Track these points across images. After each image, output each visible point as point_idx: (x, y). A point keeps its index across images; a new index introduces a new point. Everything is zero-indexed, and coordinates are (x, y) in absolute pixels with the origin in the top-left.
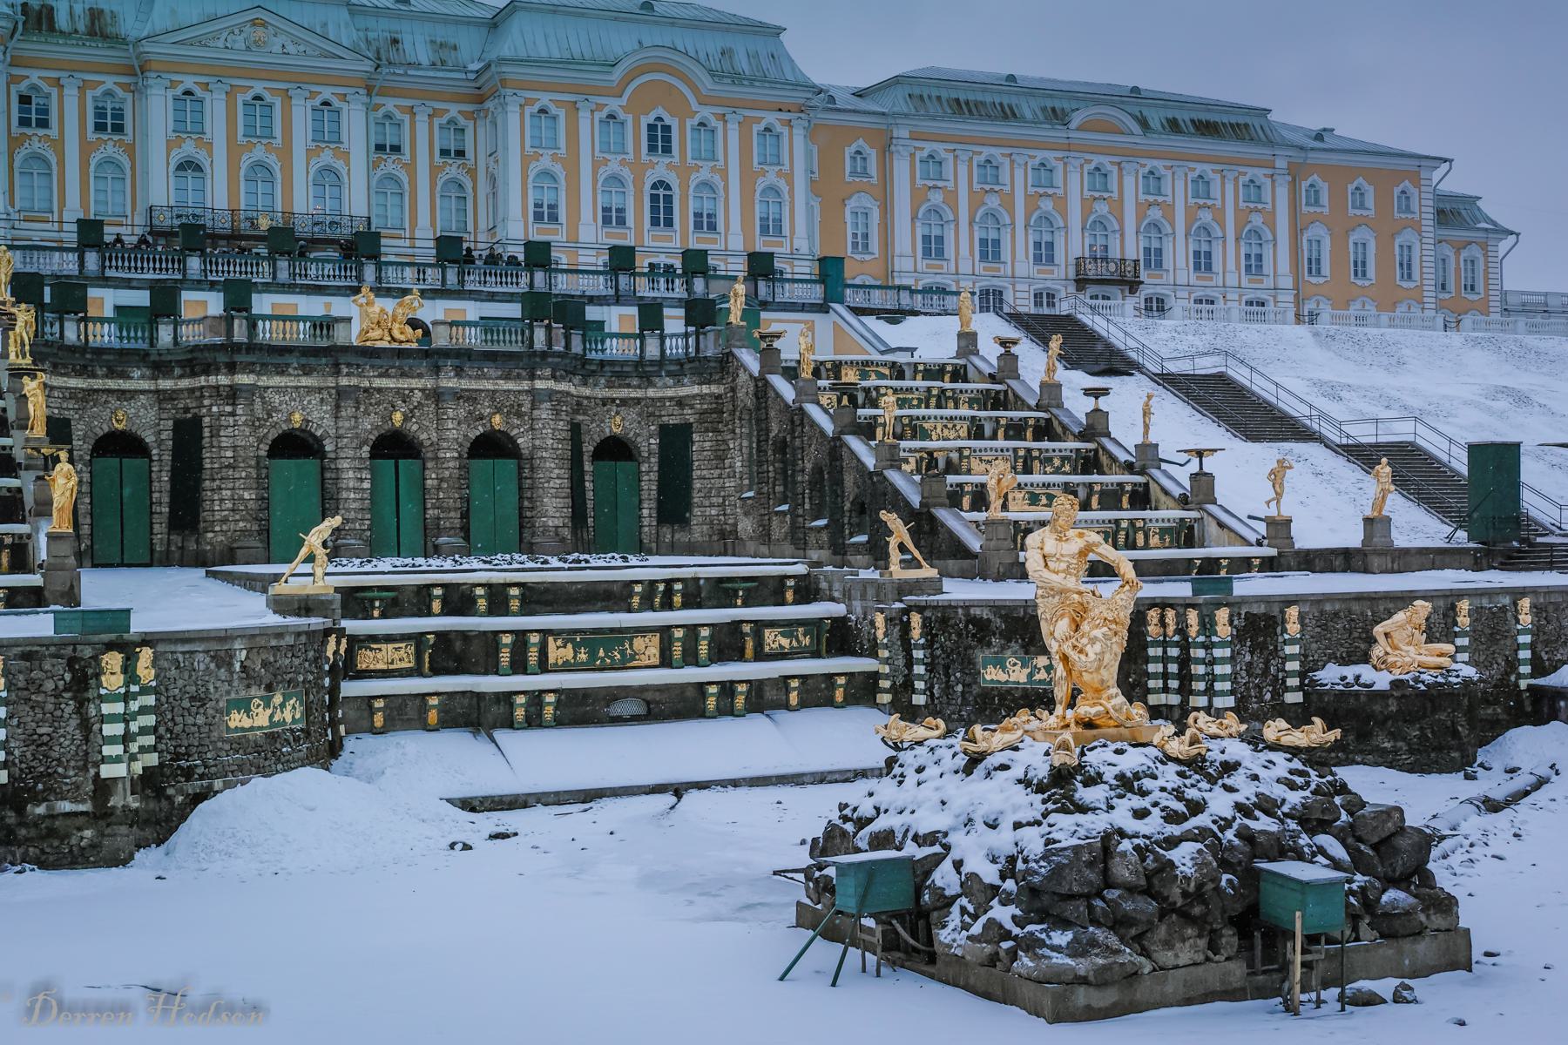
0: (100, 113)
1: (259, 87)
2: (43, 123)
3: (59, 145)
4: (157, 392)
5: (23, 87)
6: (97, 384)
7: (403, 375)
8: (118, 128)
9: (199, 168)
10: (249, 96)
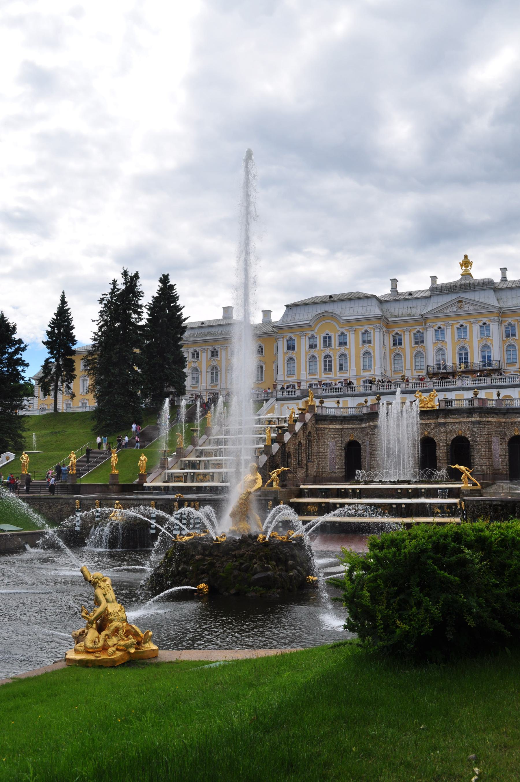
0: (416, 338)
1: (461, 323)
2: (400, 344)
3: (404, 349)
4: (362, 428)
5: (394, 334)
6: (346, 426)
7: (428, 419)
8: (422, 342)
9: (443, 350)
10: (458, 325)
